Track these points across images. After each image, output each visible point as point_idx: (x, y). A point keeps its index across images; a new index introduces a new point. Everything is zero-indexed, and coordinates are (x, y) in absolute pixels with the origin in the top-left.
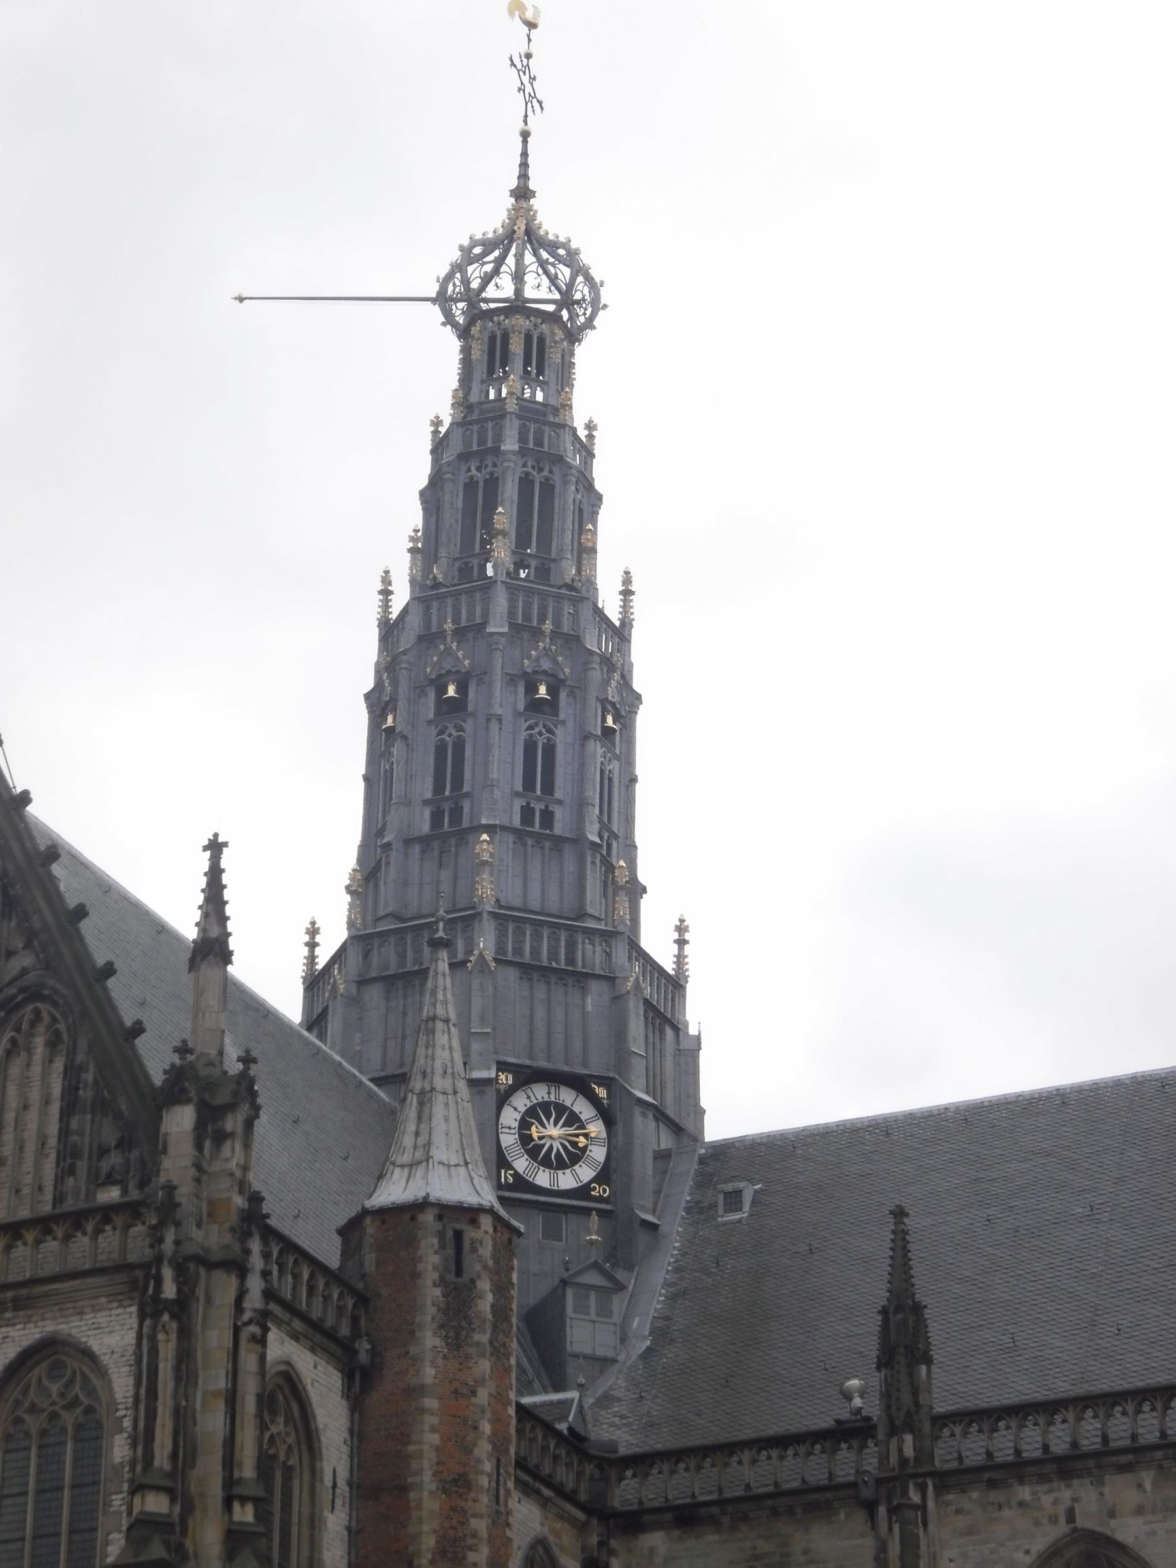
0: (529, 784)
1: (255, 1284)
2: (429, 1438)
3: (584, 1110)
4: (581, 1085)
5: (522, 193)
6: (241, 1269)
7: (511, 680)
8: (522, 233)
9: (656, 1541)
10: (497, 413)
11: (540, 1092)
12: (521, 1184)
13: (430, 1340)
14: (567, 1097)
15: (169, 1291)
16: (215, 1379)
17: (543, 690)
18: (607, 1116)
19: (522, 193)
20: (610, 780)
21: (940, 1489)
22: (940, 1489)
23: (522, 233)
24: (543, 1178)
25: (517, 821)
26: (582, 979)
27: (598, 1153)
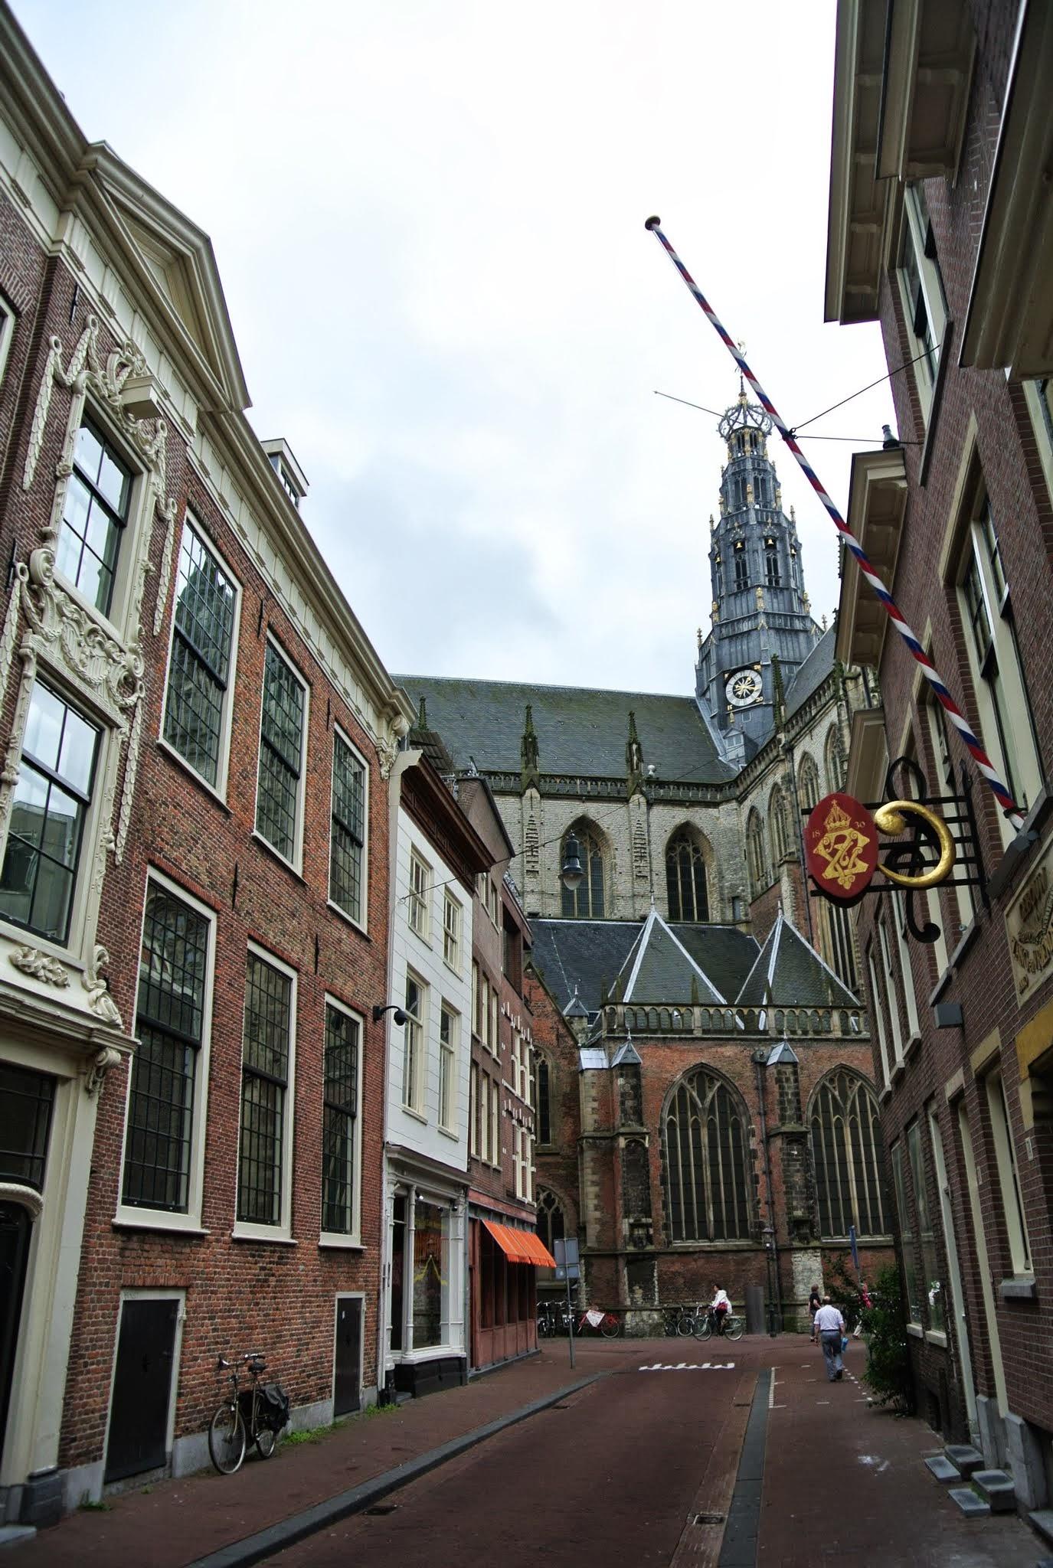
4: (750, 667)
11: (739, 675)
12: (734, 707)
14: (747, 673)
17: (739, 545)
20: (775, 561)
24: (741, 703)
27: (758, 687)
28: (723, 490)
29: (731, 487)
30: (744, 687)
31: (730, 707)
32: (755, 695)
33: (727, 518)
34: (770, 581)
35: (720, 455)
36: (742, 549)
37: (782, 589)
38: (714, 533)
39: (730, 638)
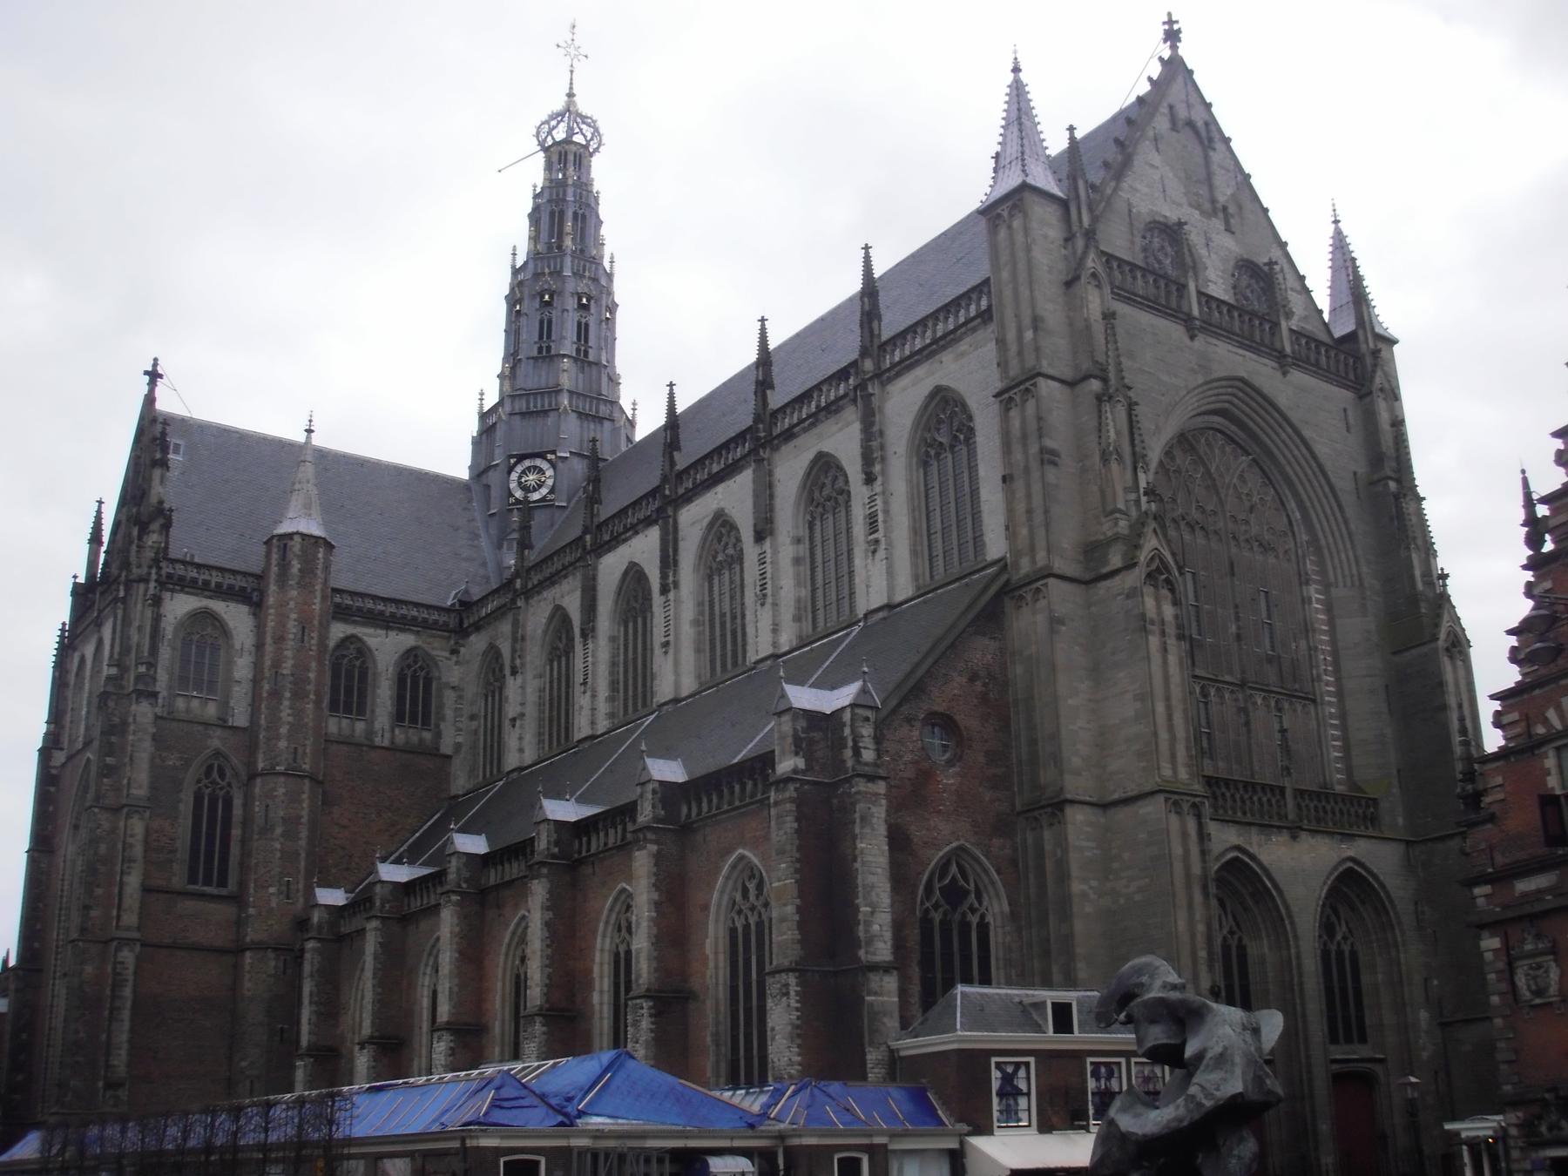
0: (541, 337)
1: (152, 585)
2: (271, 624)
3: (544, 465)
4: (542, 455)
5: (571, 95)
6: (146, 580)
7: (533, 297)
8: (569, 112)
9: (473, 638)
10: (562, 184)
11: (527, 463)
13: (273, 588)
14: (539, 462)
15: (122, 594)
16: (136, 624)
18: (553, 465)
19: (571, 95)
20: (587, 325)
21: (527, 599)
22: (527, 599)
23: (569, 112)
25: (535, 353)
26: (545, 413)
28: (535, 217)
29: (545, 218)
30: (532, 478)
31: (512, 500)
32: (544, 491)
33: (534, 256)
34: (578, 350)
35: (534, 173)
36: (548, 304)
37: (590, 364)
38: (516, 272)
39: (522, 414)
